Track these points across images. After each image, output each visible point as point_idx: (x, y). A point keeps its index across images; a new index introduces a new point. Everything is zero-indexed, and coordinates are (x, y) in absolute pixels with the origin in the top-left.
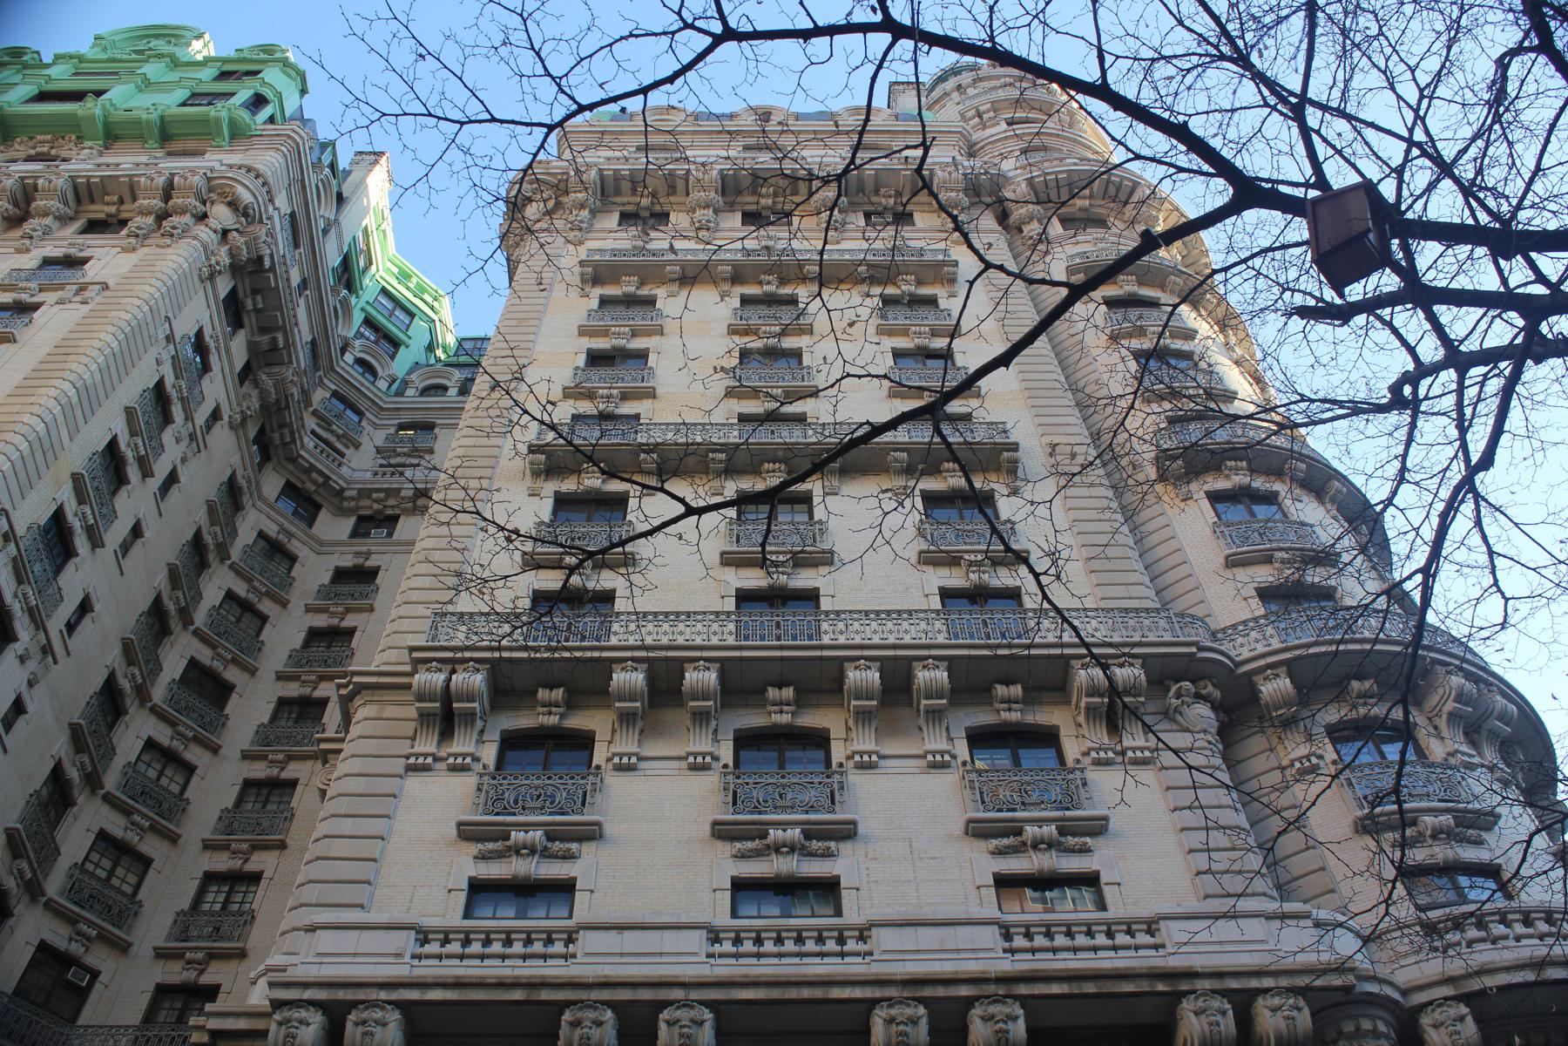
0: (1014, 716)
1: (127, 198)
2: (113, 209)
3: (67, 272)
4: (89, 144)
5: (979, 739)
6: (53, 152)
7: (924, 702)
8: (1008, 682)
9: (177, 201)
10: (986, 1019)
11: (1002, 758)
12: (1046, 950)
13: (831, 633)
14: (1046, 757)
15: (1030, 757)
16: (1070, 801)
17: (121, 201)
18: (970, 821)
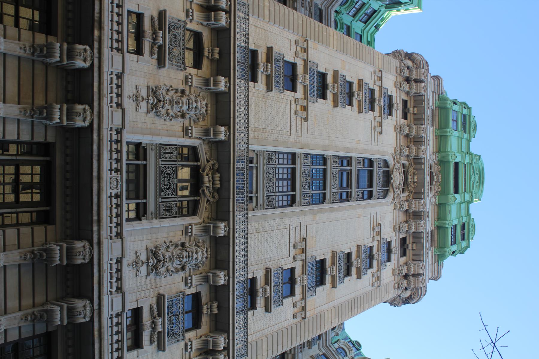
0: (205, 310)
1: (415, 252)
2: (410, 247)
3: (385, 249)
4: (437, 201)
5: (196, 297)
6: (434, 183)
7: (211, 275)
8: (218, 307)
9: (412, 279)
10: (84, 306)
11: (188, 306)
12: (112, 341)
13: (239, 216)
14: (188, 323)
15: (188, 319)
16: (172, 334)
17: (413, 250)
18: (164, 296)
